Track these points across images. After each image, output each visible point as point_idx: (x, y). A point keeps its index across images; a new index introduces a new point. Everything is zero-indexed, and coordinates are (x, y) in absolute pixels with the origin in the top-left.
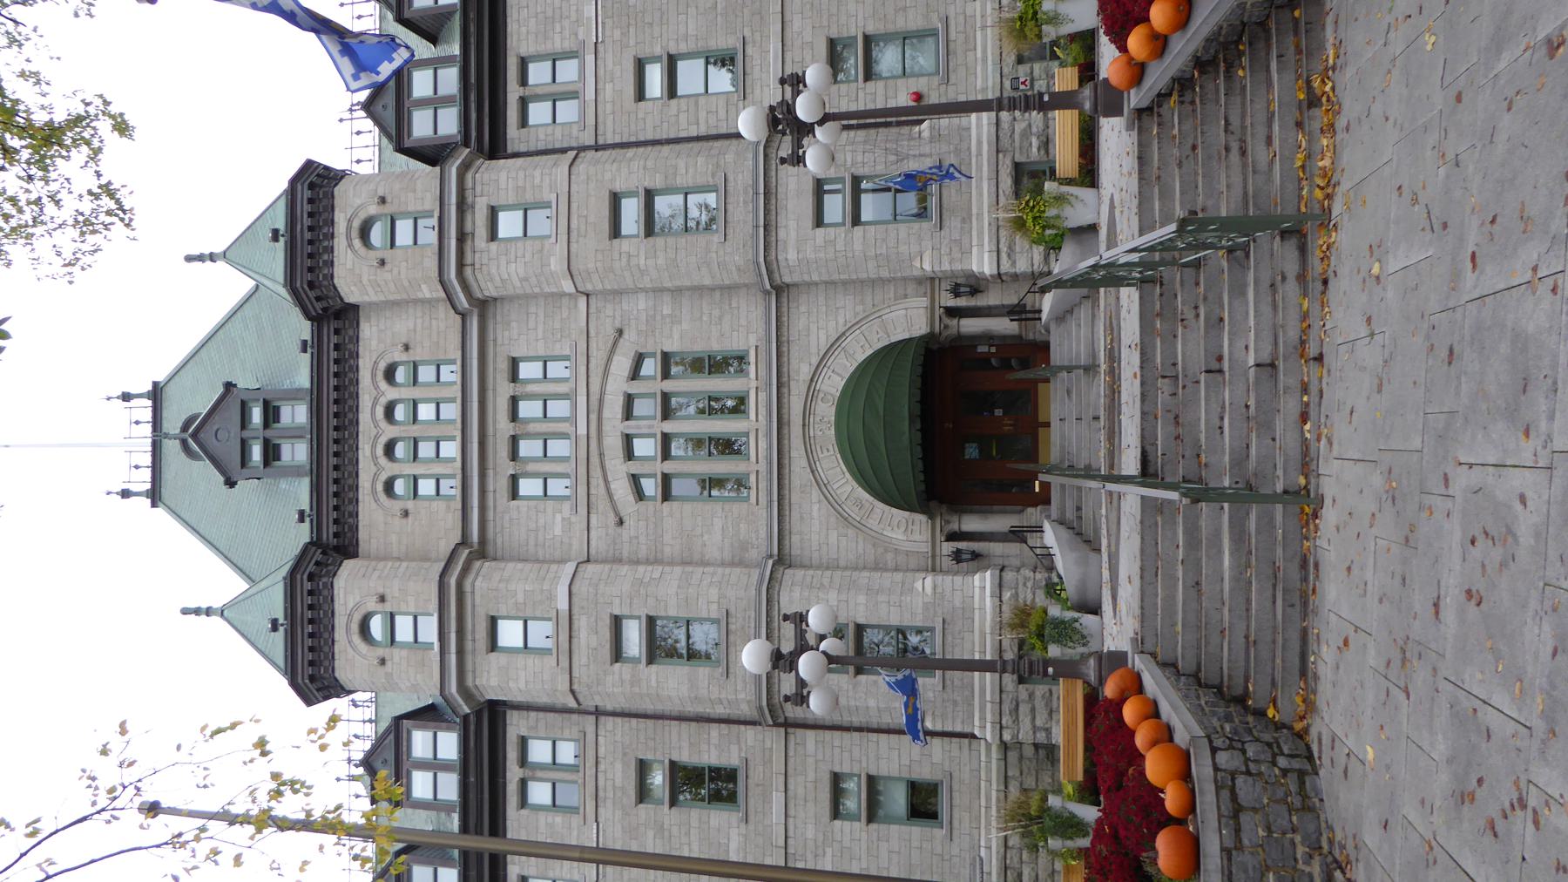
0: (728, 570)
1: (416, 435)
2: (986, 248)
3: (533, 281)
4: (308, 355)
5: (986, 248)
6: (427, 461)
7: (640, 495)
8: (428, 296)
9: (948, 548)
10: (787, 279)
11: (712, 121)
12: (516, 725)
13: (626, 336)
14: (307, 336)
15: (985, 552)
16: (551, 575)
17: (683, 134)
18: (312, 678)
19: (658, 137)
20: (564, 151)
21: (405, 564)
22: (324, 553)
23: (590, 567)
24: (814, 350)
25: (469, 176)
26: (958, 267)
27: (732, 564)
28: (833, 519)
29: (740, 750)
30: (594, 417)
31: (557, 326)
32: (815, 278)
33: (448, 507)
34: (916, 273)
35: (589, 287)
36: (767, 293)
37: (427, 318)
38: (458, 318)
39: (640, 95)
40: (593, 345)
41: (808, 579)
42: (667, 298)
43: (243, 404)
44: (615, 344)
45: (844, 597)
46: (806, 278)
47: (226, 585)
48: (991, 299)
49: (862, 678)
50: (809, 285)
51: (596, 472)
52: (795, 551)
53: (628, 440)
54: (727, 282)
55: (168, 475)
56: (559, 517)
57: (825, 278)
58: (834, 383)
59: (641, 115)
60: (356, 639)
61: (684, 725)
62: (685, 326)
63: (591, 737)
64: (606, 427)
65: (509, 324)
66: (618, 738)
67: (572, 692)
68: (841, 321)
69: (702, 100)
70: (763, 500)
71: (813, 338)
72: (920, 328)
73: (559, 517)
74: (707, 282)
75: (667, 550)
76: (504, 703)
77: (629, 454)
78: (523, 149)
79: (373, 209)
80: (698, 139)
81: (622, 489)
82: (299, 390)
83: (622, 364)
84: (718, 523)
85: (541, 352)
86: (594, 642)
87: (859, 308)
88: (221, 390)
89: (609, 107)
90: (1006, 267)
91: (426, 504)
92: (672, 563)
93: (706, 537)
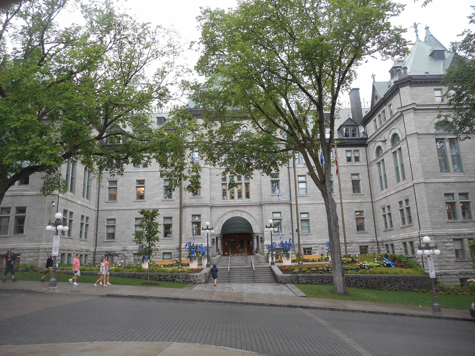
26: (265, 238)
42: (260, 183)
52: (213, 209)
58: (244, 216)
62: (255, 187)
70: (222, 203)
72: (255, 231)
84: (218, 194)
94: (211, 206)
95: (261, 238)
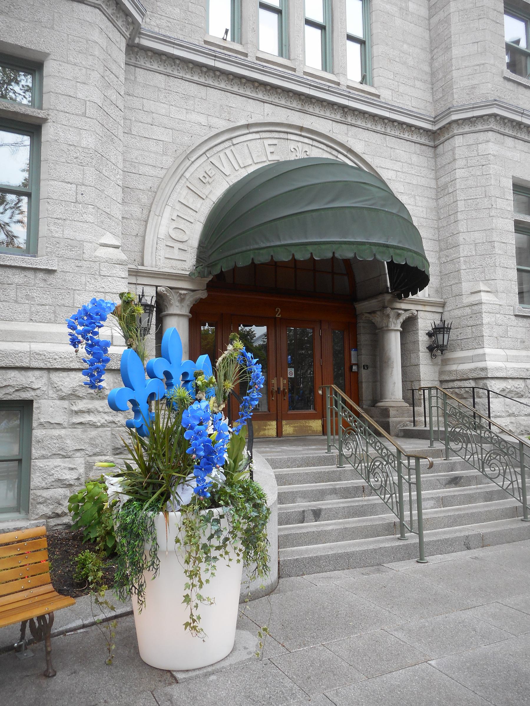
28: (186, 139)
45: (91, 111)
62: (398, 22)
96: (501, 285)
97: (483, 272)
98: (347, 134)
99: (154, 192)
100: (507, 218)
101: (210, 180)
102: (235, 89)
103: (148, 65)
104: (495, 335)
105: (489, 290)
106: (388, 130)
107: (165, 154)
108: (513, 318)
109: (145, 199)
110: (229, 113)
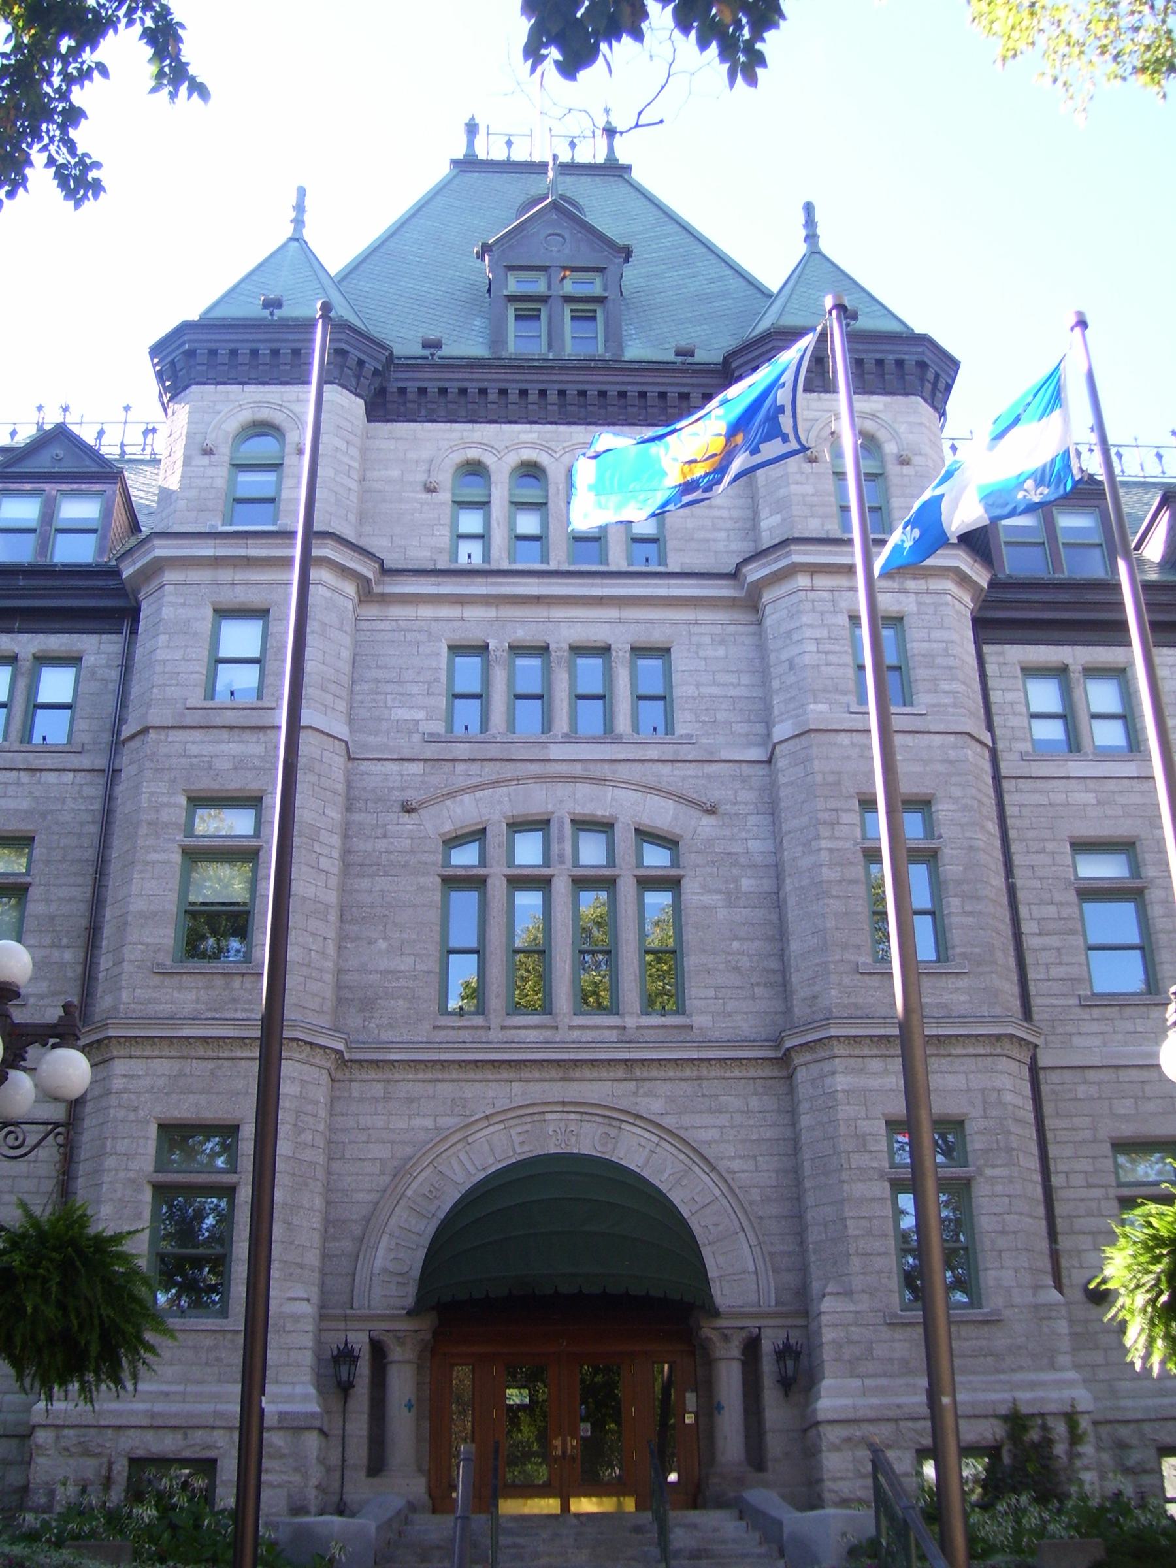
0: (328, 977)
1: (551, 505)
2: (861, 1402)
3: (791, 679)
4: (671, 357)
5: (861, 1402)
6: (512, 525)
7: (454, 841)
8: (764, 525)
9: (360, 1341)
10: (801, 1075)
11: (1045, 957)
12: (98, 649)
13: (707, 820)
14: (701, 356)
15: (352, 1404)
16: (329, 699)
17: (1023, 911)
18: (191, 354)
19: (1017, 872)
20: (990, 727)
21: (354, 486)
22: (376, 372)
23: (339, 761)
24: (687, 1120)
25: (949, 585)
26: (827, 1354)
27: (339, 986)
29: (41, 997)
30: (578, 769)
31: (721, 716)
32: (805, 1121)
33: (440, 551)
34: (816, 1286)
35: (782, 763)
36: (777, 1042)
37: (729, 524)
38: (731, 569)
39: (1082, 846)
40: (690, 770)
41: (309, 1108)
42: (767, 885)
43: (601, 270)
44: (693, 803)
46: (804, 1107)
47: (336, 250)
48: (775, 1411)
49: (147, 1195)
50: (793, 1114)
51: (490, 772)
53: (541, 824)
54: (795, 979)
55: (497, 181)
56: (421, 715)
57: (805, 1137)
58: (633, 1151)
59: (1050, 846)
60: (246, 416)
61: (82, 908)
62: (722, 913)
63: (75, 761)
64: (562, 790)
65: (722, 642)
66: (70, 804)
67: (145, 730)
68: (736, 1165)
69: (1078, 941)
71: (707, 1119)
72: (724, 1295)
73: (421, 715)
74: (794, 946)
75: (365, 883)
76: (134, 631)
77: (518, 826)
78: (990, 669)
79: (890, 448)
80: (1017, 935)
81: (464, 811)
82: (621, 347)
83: (661, 814)
84: (404, 964)
85: (678, 692)
86: (223, 764)
87: (755, 1194)
88: (621, 242)
89: (1060, 798)
90: (831, 1434)
91: (446, 520)
92: (343, 890)
93: (382, 945)
94: (342, 1061)
95: (785, 1352)
96: (857, 1282)
97: (835, 1263)
98: (635, 1094)
99: (368, 1220)
100: (870, 1180)
101: (439, 1194)
102: (471, 1075)
103: (364, 1076)
104: (847, 1357)
105: (841, 1290)
106: (704, 1072)
107: (382, 1173)
108: (884, 1328)
109: (357, 1230)
110: (464, 1107)
